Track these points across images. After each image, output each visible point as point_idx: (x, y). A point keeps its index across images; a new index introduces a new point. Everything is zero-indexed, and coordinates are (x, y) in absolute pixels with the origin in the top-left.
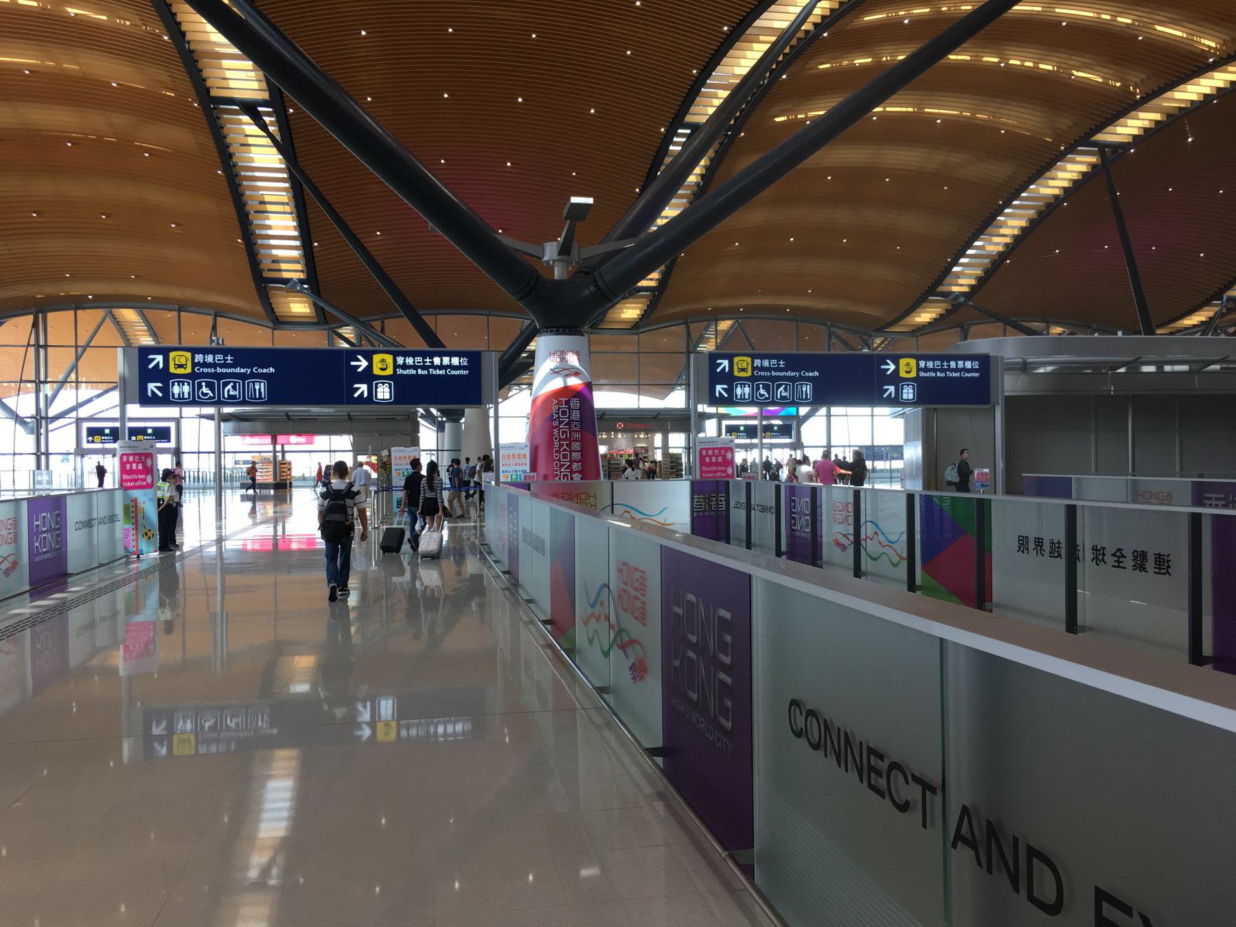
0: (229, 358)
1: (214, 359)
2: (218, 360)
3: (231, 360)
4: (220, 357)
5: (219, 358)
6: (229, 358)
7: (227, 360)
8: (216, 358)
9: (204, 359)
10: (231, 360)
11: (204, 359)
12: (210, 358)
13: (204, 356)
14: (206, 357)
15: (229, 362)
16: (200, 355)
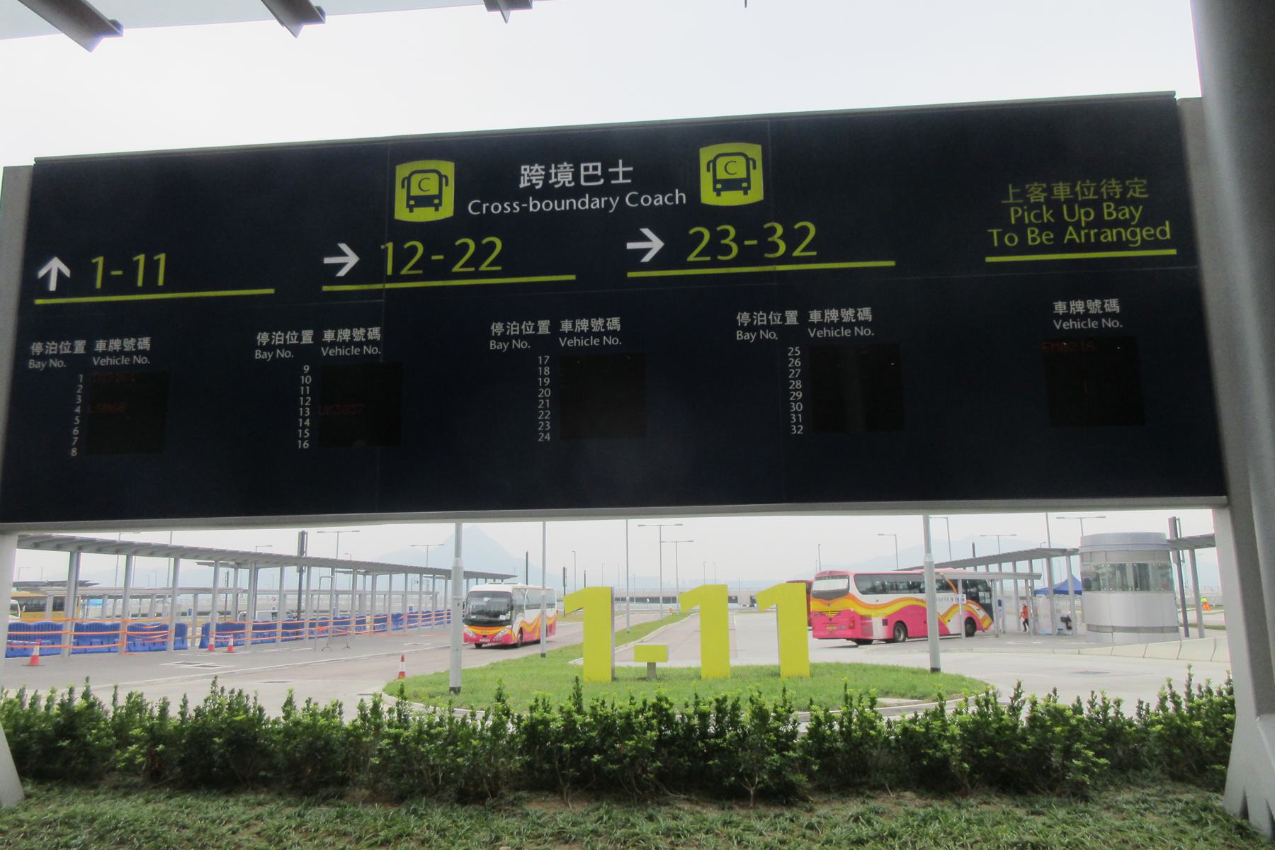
0: (621, 169)
1: (576, 176)
2: (588, 178)
3: (626, 175)
4: (592, 167)
5: (591, 172)
6: (621, 169)
7: (616, 175)
8: (583, 173)
9: (548, 176)
10: (626, 175)
11: (548, 176)
12: (563, 175)
13: (547, 170)
14: (553, 171)
15: (621, 181)
16: (536, 167)
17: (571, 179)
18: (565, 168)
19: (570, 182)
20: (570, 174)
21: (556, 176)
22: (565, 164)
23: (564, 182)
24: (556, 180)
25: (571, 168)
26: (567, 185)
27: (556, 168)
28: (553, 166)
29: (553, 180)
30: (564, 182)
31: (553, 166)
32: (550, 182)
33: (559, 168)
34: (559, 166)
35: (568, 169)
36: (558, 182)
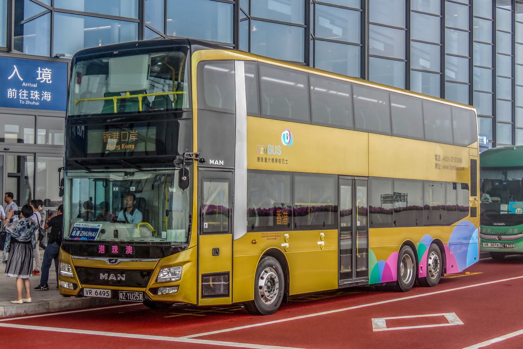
17: (50, 79)
18: (47, 71)
19: (49, 81)
20: (50, 75)
21: (41, 76)
22: (47, 69)
23: (46, 80)
24: (41, 78)
25: (50, 72)
26: (48, 82)
27: (41, 70)
28: (39, 68)
29: (39, 78)
30: (46, 80)
31: (39, 68)
32: (37, 79)
33: (43, 71)
34: (43, 69)
35: (48, 72)
36: (42, 80)
